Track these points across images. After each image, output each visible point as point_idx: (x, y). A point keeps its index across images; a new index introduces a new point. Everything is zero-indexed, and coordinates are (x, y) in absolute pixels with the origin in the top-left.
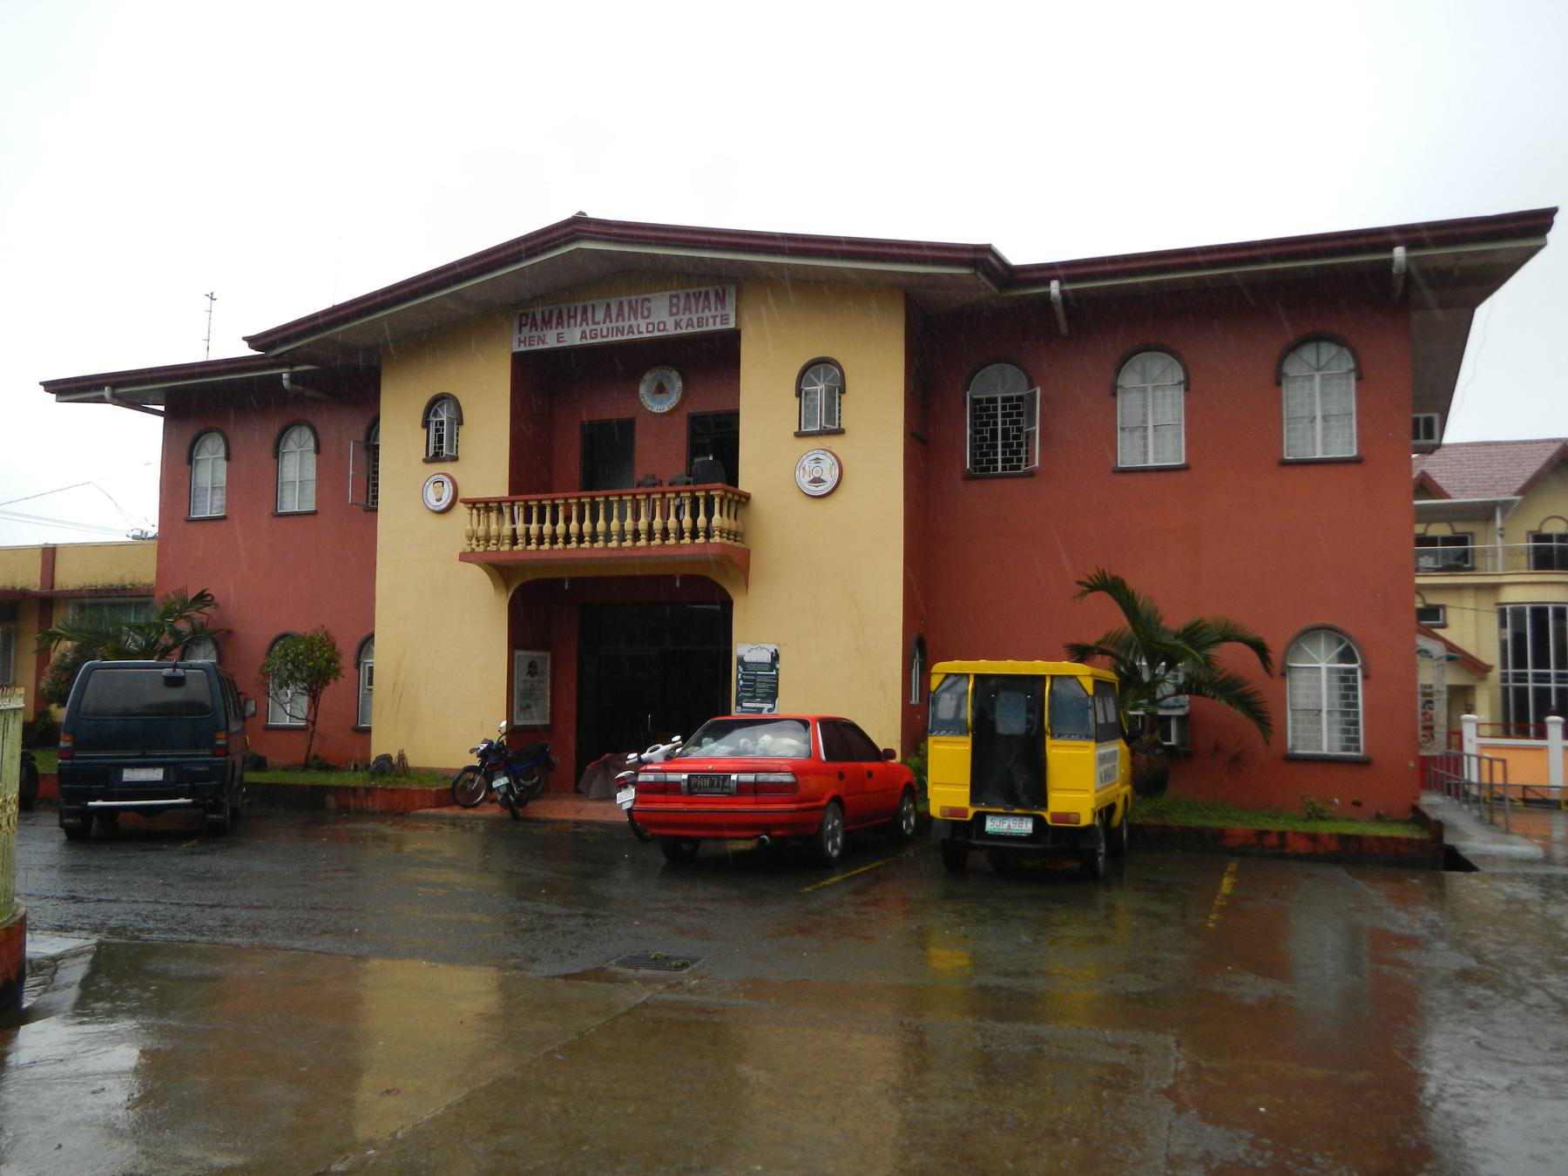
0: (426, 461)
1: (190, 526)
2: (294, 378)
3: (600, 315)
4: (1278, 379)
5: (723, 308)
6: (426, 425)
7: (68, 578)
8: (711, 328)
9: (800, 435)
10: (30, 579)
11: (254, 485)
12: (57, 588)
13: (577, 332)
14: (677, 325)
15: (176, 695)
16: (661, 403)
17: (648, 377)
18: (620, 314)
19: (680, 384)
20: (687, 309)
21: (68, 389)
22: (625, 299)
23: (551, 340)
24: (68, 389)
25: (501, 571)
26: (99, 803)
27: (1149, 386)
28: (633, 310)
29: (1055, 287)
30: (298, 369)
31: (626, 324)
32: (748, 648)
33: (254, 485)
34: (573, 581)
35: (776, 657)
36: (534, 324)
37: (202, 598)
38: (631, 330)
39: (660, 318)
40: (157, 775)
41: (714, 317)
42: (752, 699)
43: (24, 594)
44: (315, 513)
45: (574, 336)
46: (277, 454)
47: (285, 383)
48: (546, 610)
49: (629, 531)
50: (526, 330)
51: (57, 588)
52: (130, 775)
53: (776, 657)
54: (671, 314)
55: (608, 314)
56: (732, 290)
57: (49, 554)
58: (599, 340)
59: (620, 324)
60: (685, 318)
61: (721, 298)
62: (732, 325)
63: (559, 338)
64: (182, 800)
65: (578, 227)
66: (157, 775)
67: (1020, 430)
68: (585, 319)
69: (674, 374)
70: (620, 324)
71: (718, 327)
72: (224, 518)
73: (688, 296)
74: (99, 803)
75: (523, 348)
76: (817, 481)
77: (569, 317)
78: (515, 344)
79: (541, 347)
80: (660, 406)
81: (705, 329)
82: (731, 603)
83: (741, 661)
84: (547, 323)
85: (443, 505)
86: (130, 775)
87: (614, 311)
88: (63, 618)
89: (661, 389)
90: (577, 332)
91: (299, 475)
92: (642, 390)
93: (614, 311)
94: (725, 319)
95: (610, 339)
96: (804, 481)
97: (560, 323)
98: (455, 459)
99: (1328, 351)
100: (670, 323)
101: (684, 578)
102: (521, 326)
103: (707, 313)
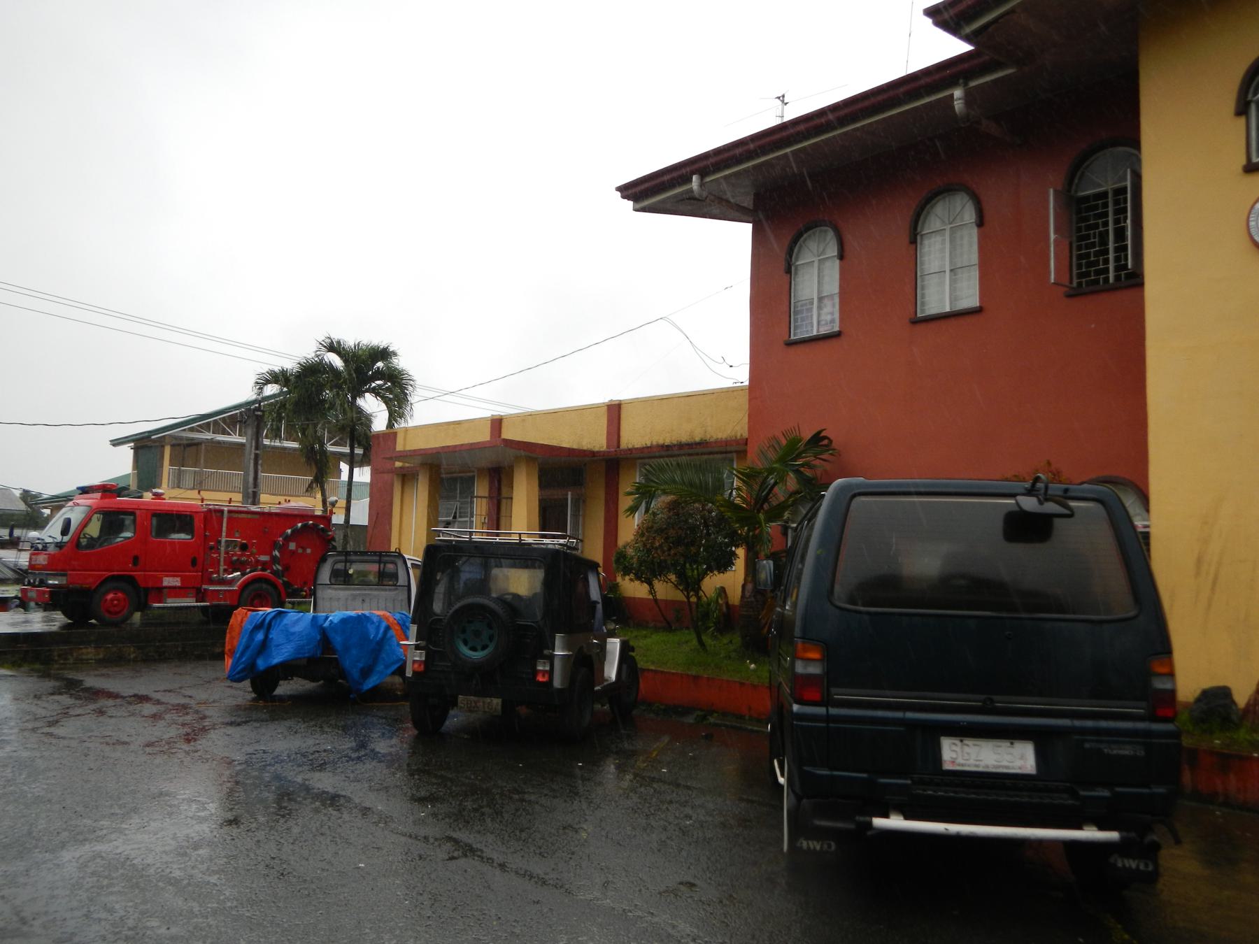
1: (792, 349)
2: (969, 98)
7: (634, 435)
10: (595, 439)
11: (881, 287)
12: (624, 445)
15: (1024, 565)
26: (896, 822)
30: (973, 84)
33: (881, 287)
37: (817, 439)
40: (1018, 758)
43: (589, 457)
44: (977, 311)
46: (914, 238)
47: (958, 105)
51: (624, 445)
52: (960, 755)
57: (615, 411)
64: (1089, 834)
66: (1018, 758)
72: (837, 335)
74: (896, 822)
86: (960, 755)
88: (630, 482)
91: (949, 267)
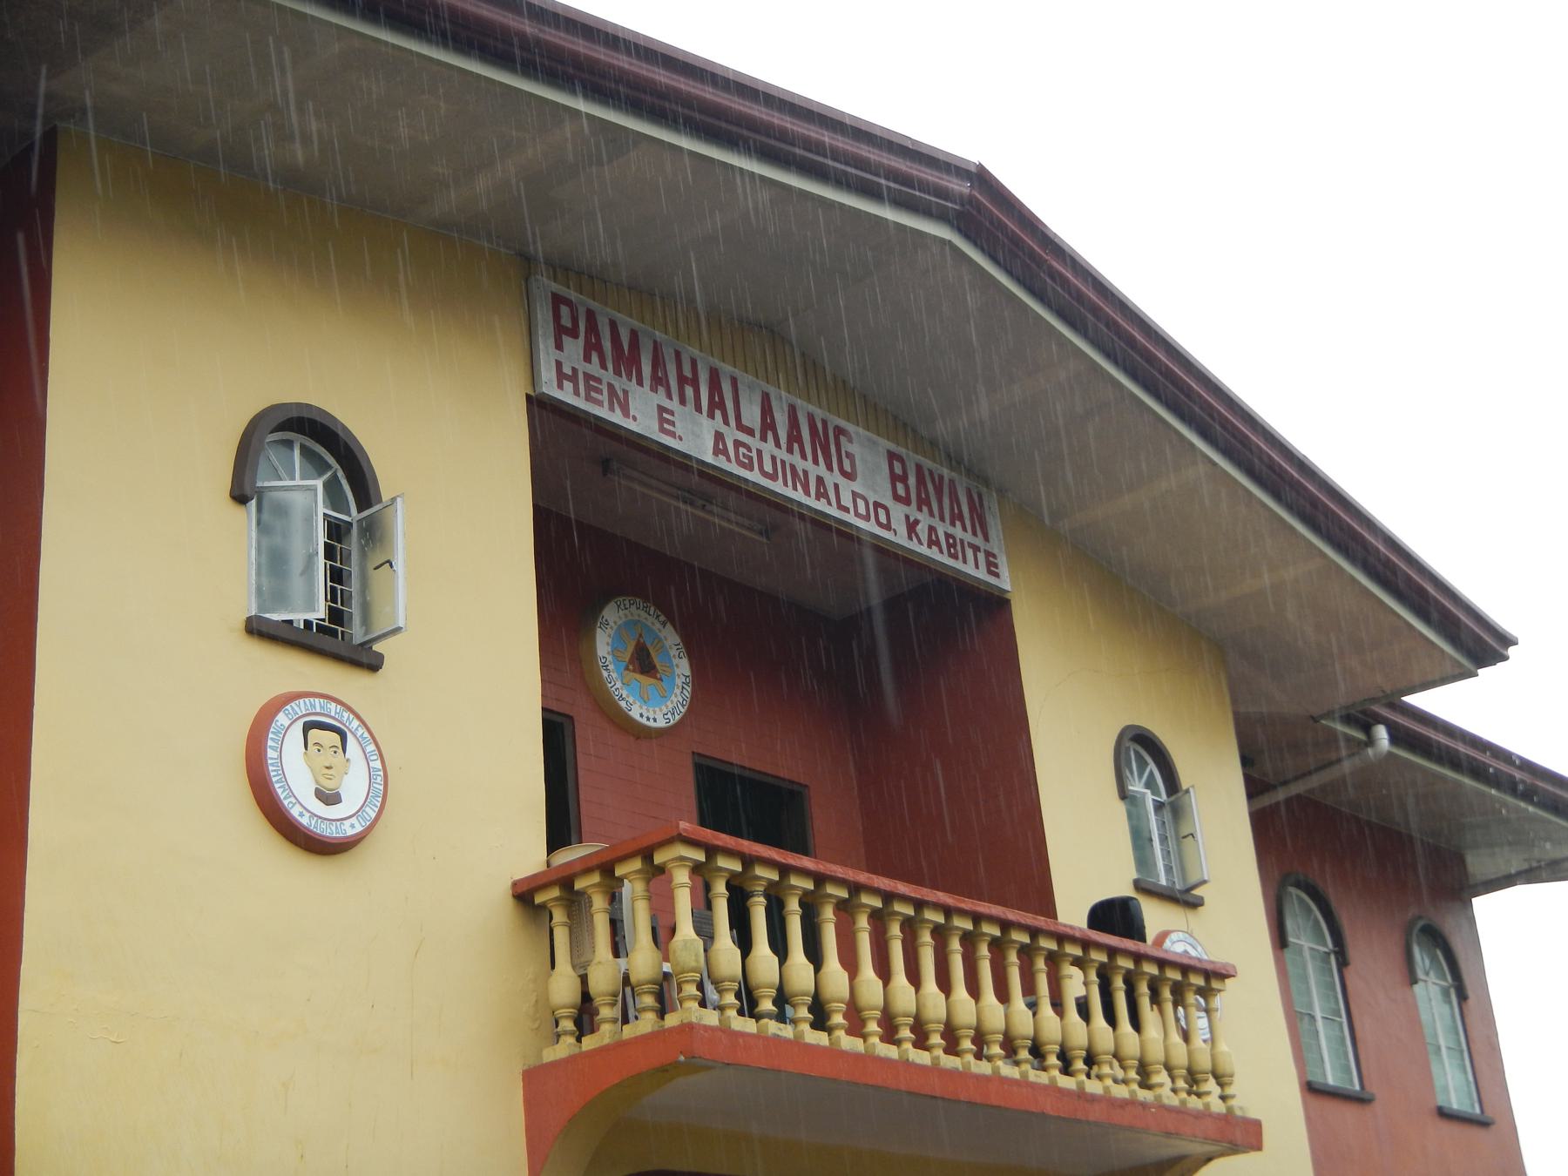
0: (258, 630)
5: (986, 539)
8: (969, 569)
14: (912, 527)
16: (645, 700)
18: (794, 437)
19: (683, 667)
41: (976, 549)
45: (696, 436)
54: (896, 497)
58: (754, 476)
62: (1005, 582)
68: (717, 405)
69: (670, 638)
71: (982, 574)
75: (566, 395)
77: (682, 380)
78: (548, 375)
79: (616, 418)
81: (958, 565)
84: (627, 361)
87: (781, 420)
89: (643, 663)
92: (603, 644)
93: (781, 420)
95: (777, 487)
102: (561, 333)
103: (958, 531)
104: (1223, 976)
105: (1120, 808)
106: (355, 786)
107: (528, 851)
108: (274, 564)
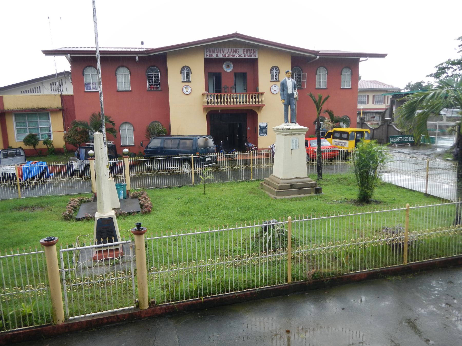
3: (226, 51)
4: (341, 74)
6: (181, 73)
8: (252, 57)
9: (271, 81)
13: (221, 55)
14: (245, 56)
17: (225, 63)
18: (231, 52)
20: (247, 52)
21: (48, 53)
22: (233, 49)
23: (215, 56)
24: (48, 53)
25: (205, 109)
27: (321, 73)
28: (235, 51)
29: (318, 57)
31: (233, 54)
32: (261, 123)
34: (221, 110)
35: (267, 125)
36: (210, 52)
38: (234, 56)
39: (241, 54)
42: (262, 133)
45: (220, 56)
47: (137, 59)
48: (214, 117)
49: (238, 100)
50: (208, 53)
53: (267, 125)
55: (228, 52)
56: (257, 50)
58: (226, 57)
59: (232, 54)
60: (247, 54)
61: (254, 51)
63: (217, 55)
65: (236, 35)
67: (300, 80)
68: (223, 52)
69: (231, 63)
70: (232, 54)
71: (254, 57)
73: (247, 50)
75: (207, 57)
76: (275, 91)
80: (228, 70)
82: (257, 115)
83: (260, 126)
85: (188, 93)
89: (228, 66)
90: (221, 55)
92: (224, 66)
94: (255, 56)
96: (272, 91)
97: (217, 52)
98: (191, 82)
99: (348, 70)
100: (243, 55)
101: (246, 110)
104: (264, 93)
105: (270, 75)
106: (189, 91)
107: (203, 91)
108: (184, 77)
